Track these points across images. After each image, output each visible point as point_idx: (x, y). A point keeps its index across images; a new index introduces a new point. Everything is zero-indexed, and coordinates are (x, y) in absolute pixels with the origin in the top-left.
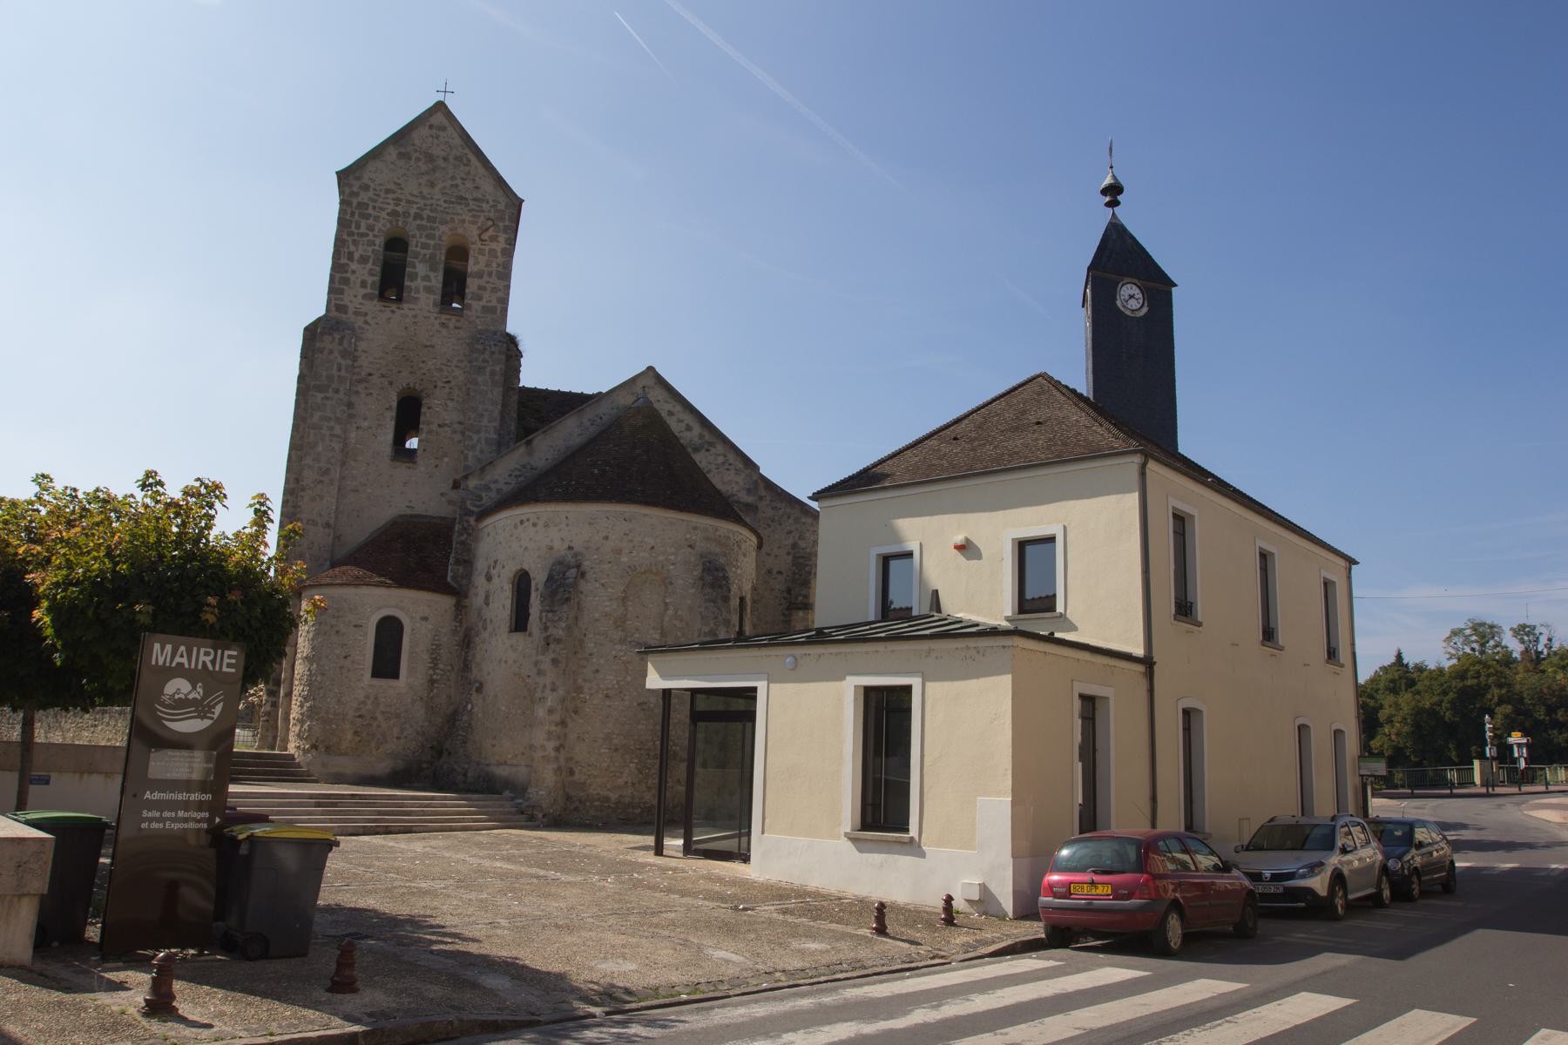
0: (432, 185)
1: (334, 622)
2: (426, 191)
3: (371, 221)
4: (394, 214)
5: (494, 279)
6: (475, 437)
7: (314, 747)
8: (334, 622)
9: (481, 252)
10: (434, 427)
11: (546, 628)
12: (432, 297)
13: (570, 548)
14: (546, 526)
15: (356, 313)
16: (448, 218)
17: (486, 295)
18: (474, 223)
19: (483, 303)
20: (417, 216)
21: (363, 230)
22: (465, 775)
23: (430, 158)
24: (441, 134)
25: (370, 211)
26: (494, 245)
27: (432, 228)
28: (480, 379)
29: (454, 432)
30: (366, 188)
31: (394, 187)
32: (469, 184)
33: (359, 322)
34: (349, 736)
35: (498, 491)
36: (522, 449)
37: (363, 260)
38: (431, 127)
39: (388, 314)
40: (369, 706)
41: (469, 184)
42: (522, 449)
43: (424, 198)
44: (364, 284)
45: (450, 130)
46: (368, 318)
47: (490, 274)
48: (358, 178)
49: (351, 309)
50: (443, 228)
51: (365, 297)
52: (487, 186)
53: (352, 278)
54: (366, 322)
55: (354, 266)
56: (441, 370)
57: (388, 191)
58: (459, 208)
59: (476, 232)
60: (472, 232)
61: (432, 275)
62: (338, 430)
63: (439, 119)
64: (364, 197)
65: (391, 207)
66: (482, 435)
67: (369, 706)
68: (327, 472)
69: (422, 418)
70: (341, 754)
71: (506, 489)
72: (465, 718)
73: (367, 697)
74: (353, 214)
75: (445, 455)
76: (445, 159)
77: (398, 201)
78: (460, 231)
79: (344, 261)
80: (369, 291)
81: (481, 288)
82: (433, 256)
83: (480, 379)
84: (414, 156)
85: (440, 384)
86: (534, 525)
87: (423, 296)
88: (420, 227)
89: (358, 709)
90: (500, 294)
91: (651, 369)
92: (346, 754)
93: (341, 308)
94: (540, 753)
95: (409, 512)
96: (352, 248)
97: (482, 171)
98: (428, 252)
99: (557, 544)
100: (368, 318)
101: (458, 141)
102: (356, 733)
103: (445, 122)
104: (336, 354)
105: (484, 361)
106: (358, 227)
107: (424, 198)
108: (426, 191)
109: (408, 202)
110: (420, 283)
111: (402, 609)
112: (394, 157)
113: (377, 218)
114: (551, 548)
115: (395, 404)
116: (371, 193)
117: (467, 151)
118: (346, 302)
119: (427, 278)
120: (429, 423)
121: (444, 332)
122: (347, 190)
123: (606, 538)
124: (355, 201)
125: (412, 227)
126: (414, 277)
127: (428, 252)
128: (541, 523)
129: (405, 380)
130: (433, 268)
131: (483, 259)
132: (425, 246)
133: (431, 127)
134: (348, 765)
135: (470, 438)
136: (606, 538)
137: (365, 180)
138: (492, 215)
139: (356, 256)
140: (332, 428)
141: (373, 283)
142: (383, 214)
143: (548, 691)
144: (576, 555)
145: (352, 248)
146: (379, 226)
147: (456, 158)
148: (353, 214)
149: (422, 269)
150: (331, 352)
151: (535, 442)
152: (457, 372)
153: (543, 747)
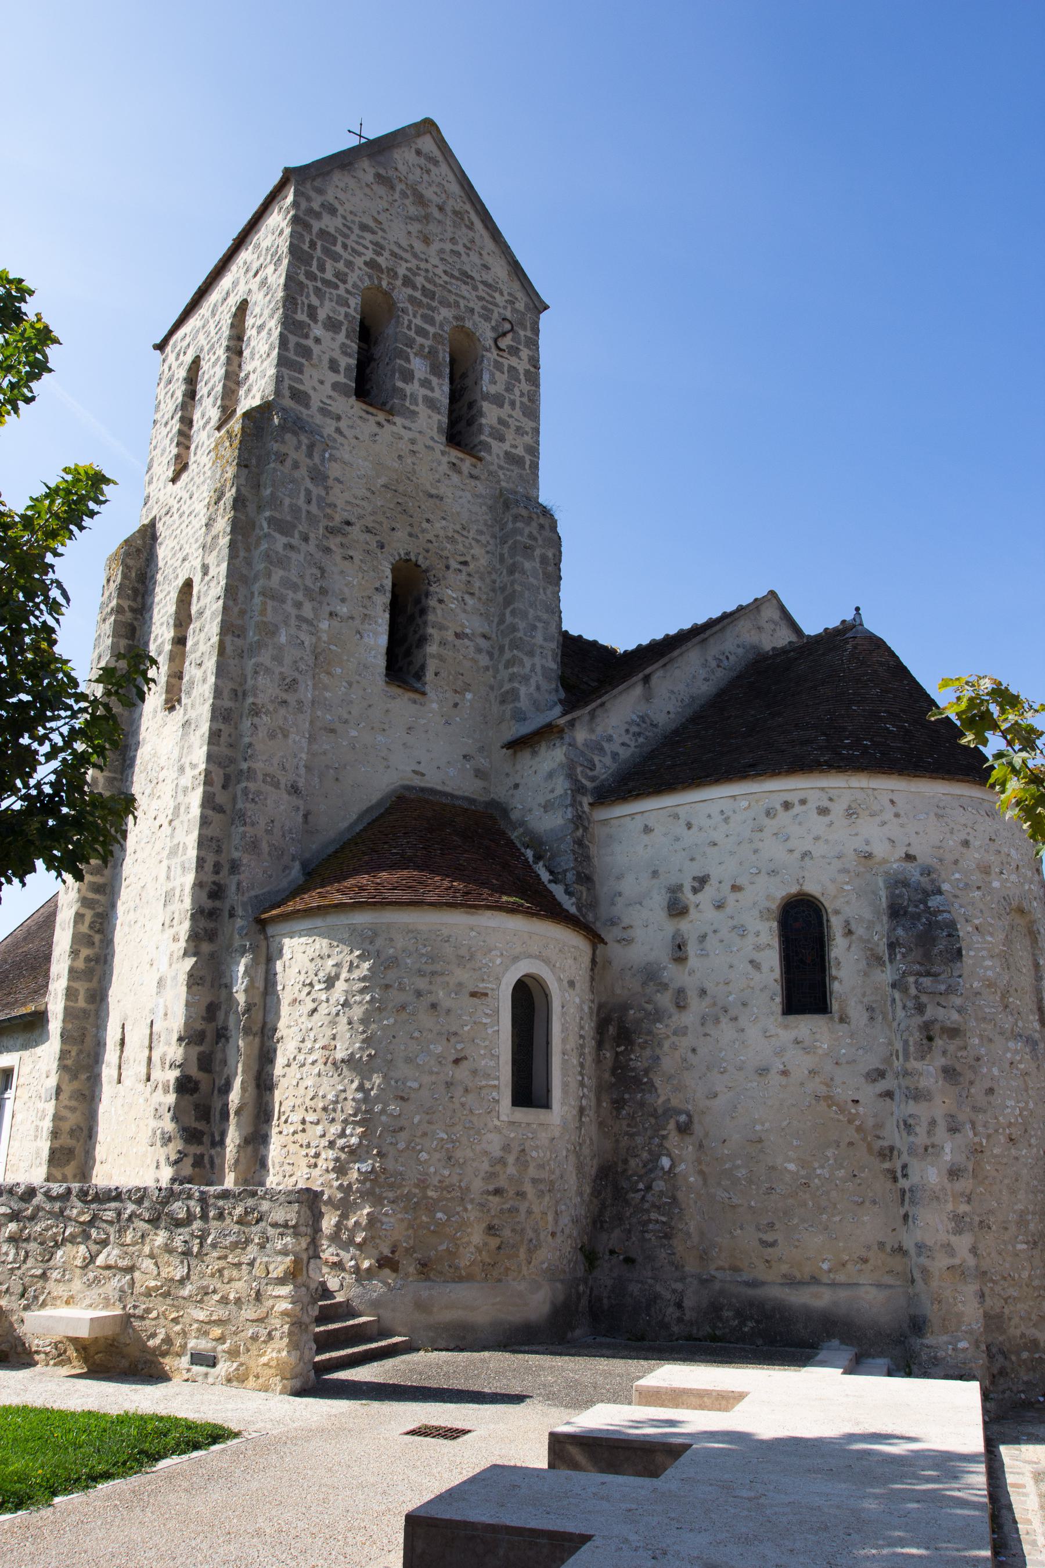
0: (426, 241)
1: (422, 984)
2: (419, 246)
3: (341, 266)
4: (371, 264)
5: (517, 413)
6: (528, 662)
7: (386, 1263)
8: (422, 984)
9: (498, 366)
10: (449, 636)
11: (920, 1009)
12: (436, 417)
13: (909, 858)
14: (851, 813)
15: (324, 411)
16: (452, 298)
17: (510, 435)
18: (487, 319)
19: (506, 446)
20: (407, 282)
21: (329, 275)
22: (679, 1305)
23: (420, 200)
24: (432, 167)
25: (339, 249)
26: (514, 361)
27: (433, 309)
28: (527, 565)
29: (479, 650)
30: (333, 211)
31: (372, 224)
32: (474, 257)
33: (329, 428)
34: (476, 1236)
35: (615, 755)
36: (638, 690)
37: (332, 325)
38: (418, 153)
39: (371, 426)
40: (511, 1170)
41: (474, 257)
42: (638, 690)
43: (415, 256)
44: (334, 366)
45: (444, 168)
46: (343, 425)
47: (513, 404)
48: (320, 191)
49: (315, 404)
50: (445, 313)
51: (335, 386)
52: (500, 270)
53: (316, 349)
54: (338, 430)
55: (318, 331)
56: (452, 540)
57: (364, 227)
58: (465, 290)
59: (490, 335)
60: (486, 333)
61: (435, 380)
62: (307, 611)
63: (426, 143)
64: (329, 223)
65: (369, 255)
66: (537, 660)
67: (511, 1170)
68: (292, 685)
69: (431, 617)
70: (461, 1279)
71: (624, 753)
72: (659, 1185)
73: (506, 1148)
74: (313, 245)
75: (467, 688)
76: (441, 209)
77: (379, 249)
78: (469, 324)
79: (302, 316)
80: (341, 378)
81: (501, 421)
82: (432, 353)
83: (527, 565)
84: (400, 187)
85: (454, 565)
86: (823, 811)
87: (421, 409)
88: (412, 299)
89: (491, 1176)
90: (528, 439)
91: (772, 593)
92: (469, 1278)
93: (300, 396)
94: (942, 1262)
95: (417, 782)
96: (315, 301)
97: (489, 245)
98: (427, 343)
99: (880, 850)
100: (343, 425)
101: (454, 188)
102: (491, 1229)
103: (436, 153)
104: (303, 472)
105: (531, 536)
106: (322, 268)
107: (415, 256)
108: (419, 246)
109: (394, 254)
110: (413, 388)
111: (547, 961)
112: (370, 178)
113: (349, 264)
114: (869, 856)
115: (388, 583)
116: (338, 222)
117: (468, 207)
118: (306, 387)
119: (425, 383)
120: (442, 628)
121: (455, 478)
122: (304, 205)
123: (966, 843)
124: (316, 226)
125: (401, 294)
126: (408, 376)
127: (427, 343)
128: (838, 809)
129: (401, 544)
130: (435, 370)
131: (502, 378)
132: (421, 332)
133: (418, 153)
134: (475, 1303)
135: (522, 663)
136: (966, 843)
137: (330, 197)
138: (508, 314)
139: (322, 315)
140: (298, 605)
141: (348, 368)
142: (359, 262)
143: (941, 1131)
144: (927, 871)
145: (315, 301)
146: (353, 278)
147: (456, 213)
148: (313, 245)
149: (419, 366)
150: (296, 466)
151: (654, 680)
152: (477, 551)
153: (949, 1249)
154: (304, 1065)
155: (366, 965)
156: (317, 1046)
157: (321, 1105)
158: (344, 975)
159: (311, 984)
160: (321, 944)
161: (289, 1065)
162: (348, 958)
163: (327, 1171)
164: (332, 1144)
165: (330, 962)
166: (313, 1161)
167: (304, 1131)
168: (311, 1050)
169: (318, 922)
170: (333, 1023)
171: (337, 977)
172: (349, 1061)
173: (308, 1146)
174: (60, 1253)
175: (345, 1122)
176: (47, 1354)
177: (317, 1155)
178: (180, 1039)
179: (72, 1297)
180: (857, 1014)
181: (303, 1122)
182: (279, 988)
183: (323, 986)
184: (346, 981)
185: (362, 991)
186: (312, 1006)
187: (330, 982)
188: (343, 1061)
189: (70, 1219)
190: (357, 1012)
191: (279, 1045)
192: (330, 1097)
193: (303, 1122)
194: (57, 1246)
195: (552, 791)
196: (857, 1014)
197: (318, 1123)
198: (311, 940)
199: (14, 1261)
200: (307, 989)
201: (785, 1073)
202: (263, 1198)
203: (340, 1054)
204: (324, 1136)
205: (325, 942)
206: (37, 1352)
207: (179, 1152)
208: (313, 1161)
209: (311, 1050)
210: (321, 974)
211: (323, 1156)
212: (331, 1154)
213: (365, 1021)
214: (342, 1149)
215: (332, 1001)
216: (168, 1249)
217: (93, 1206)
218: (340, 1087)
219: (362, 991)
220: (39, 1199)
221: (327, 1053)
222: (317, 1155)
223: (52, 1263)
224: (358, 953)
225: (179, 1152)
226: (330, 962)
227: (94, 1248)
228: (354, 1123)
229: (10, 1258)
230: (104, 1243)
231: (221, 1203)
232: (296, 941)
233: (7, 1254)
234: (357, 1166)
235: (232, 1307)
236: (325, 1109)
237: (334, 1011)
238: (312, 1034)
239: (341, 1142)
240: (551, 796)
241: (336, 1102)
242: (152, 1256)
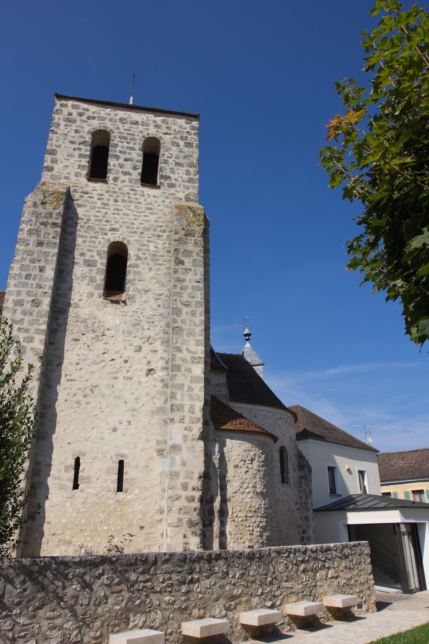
154: (243, 493)
155: (263, 456)
156: (250, 486)
157: (254, 509)
158: (257, 459)
159: (245, 461)
160: (247, 445)
161: (236, 493)
162: (258, 453)
163: (257, 536)
164: (258, 526)
165: (252, 453)
166: (251, 532)
167: (246, 520)
168: (247, 487)
169: (247, 436)
170: (255, 477)
171: (254, 459)
172: (261, 493)
173: (249, 526)
174: (318, 575)
175: (261, 517)
176: (324, 618)
177: (253, 530)
178: (200, 477)
179: (325, 592)
180: (292, 485)
181: (246, 517)
182: (227, 459)
183: (250, 462)
184: (258, 461)
185: (263, 466)
186: (247, 469)
187: (252, 460)
188: (260, 493)
189: (319, 559)
190: (261, 474)
191: (228, 484)
192: (257, 506)
193: (246, 517)
194: (317, 572)
195: (219, 391)
196: (292, 485)
197: (252, 517)
198: (243, 443)
199: (306, 581)
200: (243, 463)
201: (283, 501)
202: (362, 546)
203: (259, 490)
204: (255, 522)
205: (250, 445)
206: (321, 618)
207: (201, 530)
208: (251, 532)
209: (247, 487)
210: (249, 458)
211: (255, 530)
212: (259, 529)
213: (263, 478)
214: (261, 527)
215: (254, 468)
216: (346, 567)
217: (325, 553)
218: (260, 503)
219: (263, 466)
220: (309, 552)
221: (254, 489)
222: (253, 530)
223: (316, 579)
224: (261, 451)
225: (201, 530)
226: (252, 453)
227: (327, 570)
228: (264, 517)
229: (304, 580)
230: (329, 568)
231: (354, 548)
232: (234, 441)
233: (303, 578)
234: (265, 534)
235: (362, 585)
236: (255, 511)
237: (255, 472)
238: (247, 481)
239: (261, 525)
240: (218, 393)
241: (258, 509)
242: (342, 571)
